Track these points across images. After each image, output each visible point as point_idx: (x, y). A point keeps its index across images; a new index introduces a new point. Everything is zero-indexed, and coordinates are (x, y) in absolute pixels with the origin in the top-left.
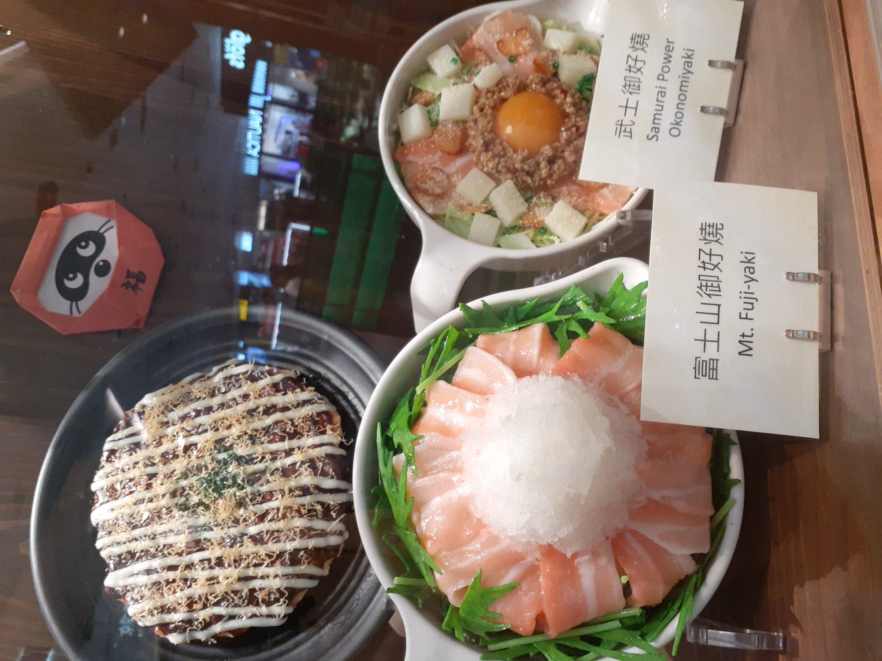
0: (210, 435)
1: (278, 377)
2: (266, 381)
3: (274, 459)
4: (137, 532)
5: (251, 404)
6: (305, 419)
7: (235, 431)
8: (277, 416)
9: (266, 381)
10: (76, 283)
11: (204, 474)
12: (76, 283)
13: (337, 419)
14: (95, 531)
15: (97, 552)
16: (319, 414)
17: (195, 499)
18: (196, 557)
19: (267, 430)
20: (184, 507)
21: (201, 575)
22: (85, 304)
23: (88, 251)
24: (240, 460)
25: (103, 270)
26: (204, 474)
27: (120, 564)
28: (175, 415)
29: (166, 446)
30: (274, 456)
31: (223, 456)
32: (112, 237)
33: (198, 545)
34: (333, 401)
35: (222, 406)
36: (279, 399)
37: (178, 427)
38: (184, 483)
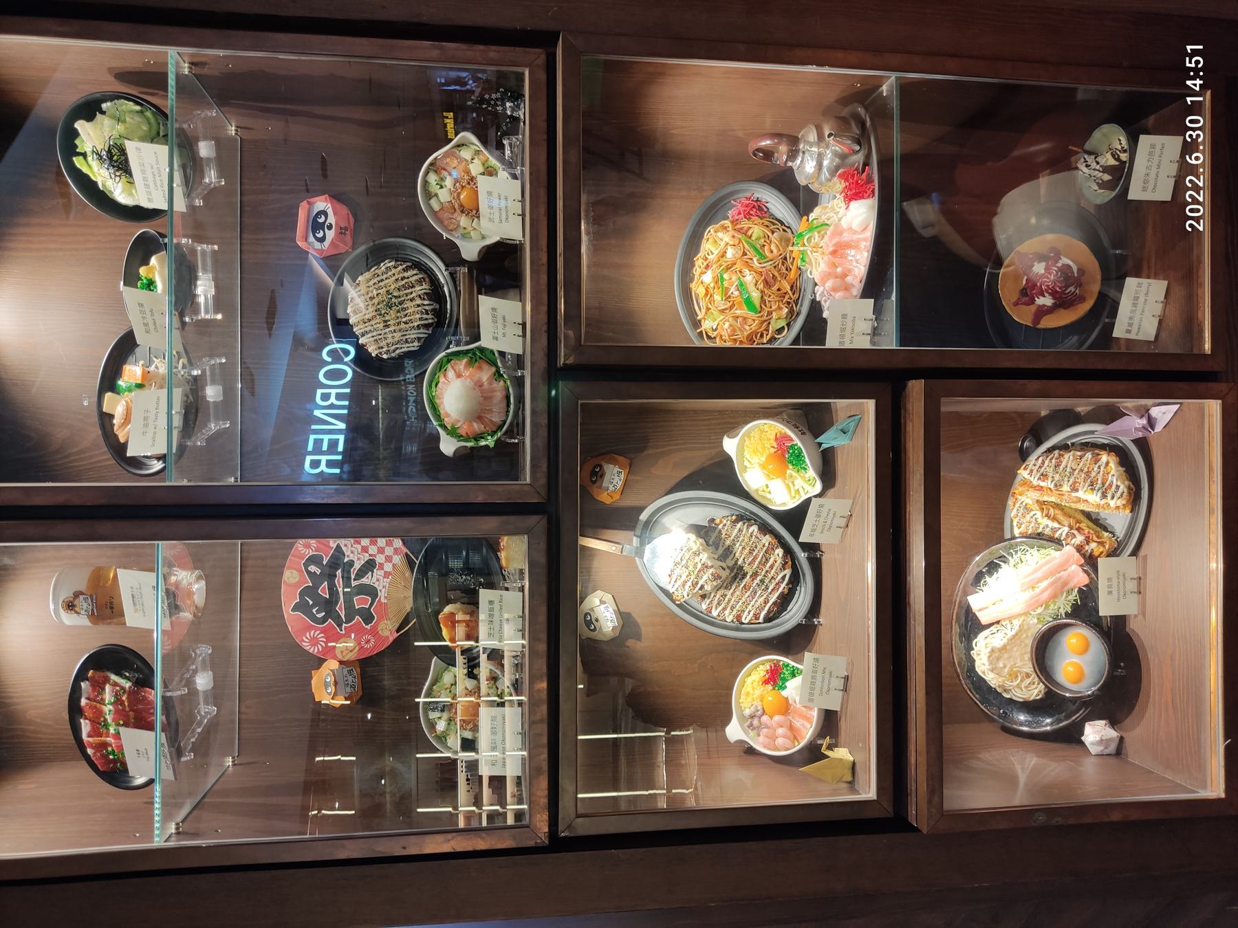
0: (384, 289)
1: (404, 266)
2: (400, 268)
3: (407, 296)
4: (366, 324)
5: (396, 277)
6: (416, 281)
7: (392, 287)
8: (406, 280)
9: (400, 268)
10: (320, 235)
11: (385, 303)
12: (320, 235)
13: (427, 279)
14: (352, 326)
15: (355, 333)
16: (420, 279)
17: (383, 312)
18: (387, 330)
19: (403, 286)
20: (380, 315)
21: (390, 336)
22: (327, 243)
23: (321, 220)
24: (395, 297)
25: (330, 227)
26: (385, 303)
27: (363, 335)
28: (371, 283)
29: (370, 295)
30: (407, 295)
31: (390, 296)
32: (330, 212)
33: (387, 326)
34: (427, 273)
35: (386, 278)
36: (406, 274)
37: (373, 287)
38: (378, 307)
